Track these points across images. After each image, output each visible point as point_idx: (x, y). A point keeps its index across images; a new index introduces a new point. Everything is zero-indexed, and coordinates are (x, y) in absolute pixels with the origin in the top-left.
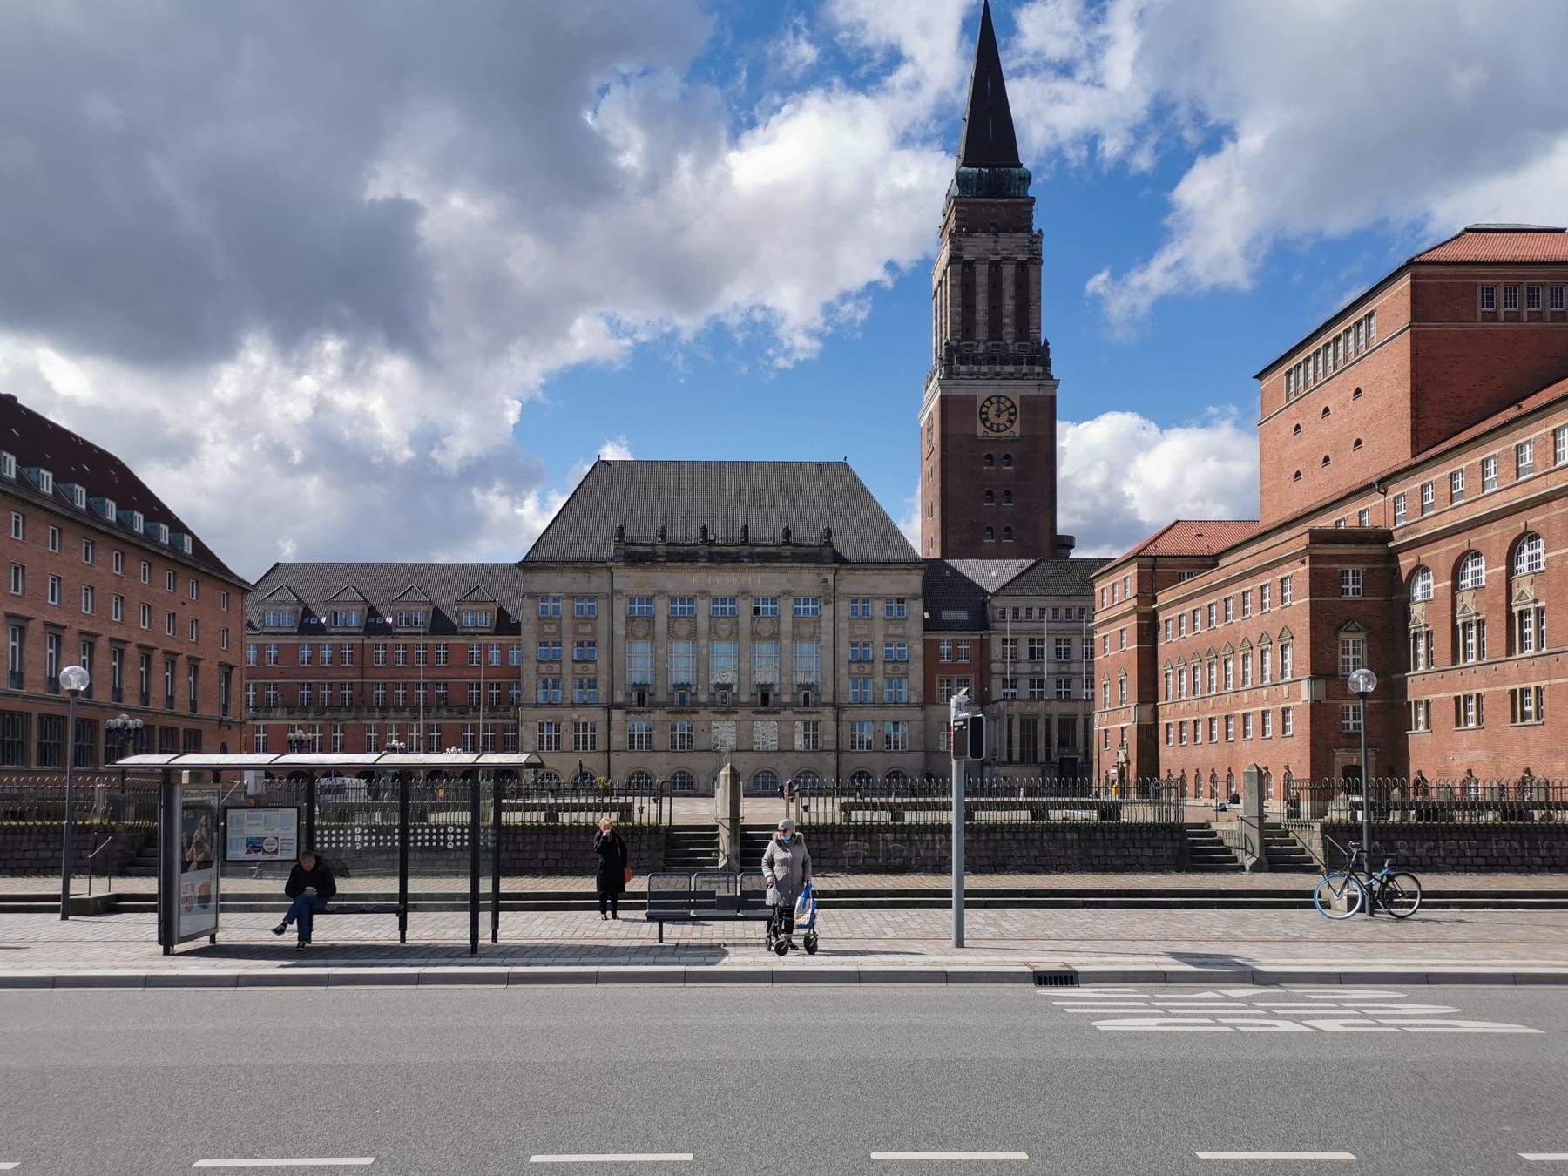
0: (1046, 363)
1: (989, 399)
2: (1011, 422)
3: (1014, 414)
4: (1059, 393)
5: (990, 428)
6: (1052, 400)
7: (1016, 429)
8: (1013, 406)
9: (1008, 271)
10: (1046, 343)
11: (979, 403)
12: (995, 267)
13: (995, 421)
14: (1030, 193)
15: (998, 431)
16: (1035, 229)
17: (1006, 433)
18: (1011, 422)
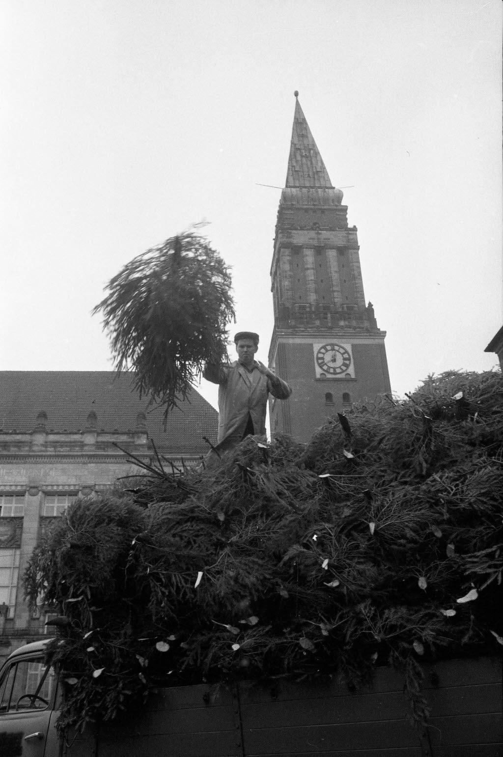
0: (373, 322)
1: (324, 347)
2: (347, 366)
3: (349, 359)
4: (388, 342)
5: (326, 371)
6: (382, 348)
7: (351, 370)
8: (346, 352)
9: (332, 254)
10: (370, 305)
11: (316, 350)
12: (320, 250)
13: (331, 365)
14: (343, 203)
15: (335, 373)
16: (350, 226)
17: (342, 376)
18: (344, 364)
